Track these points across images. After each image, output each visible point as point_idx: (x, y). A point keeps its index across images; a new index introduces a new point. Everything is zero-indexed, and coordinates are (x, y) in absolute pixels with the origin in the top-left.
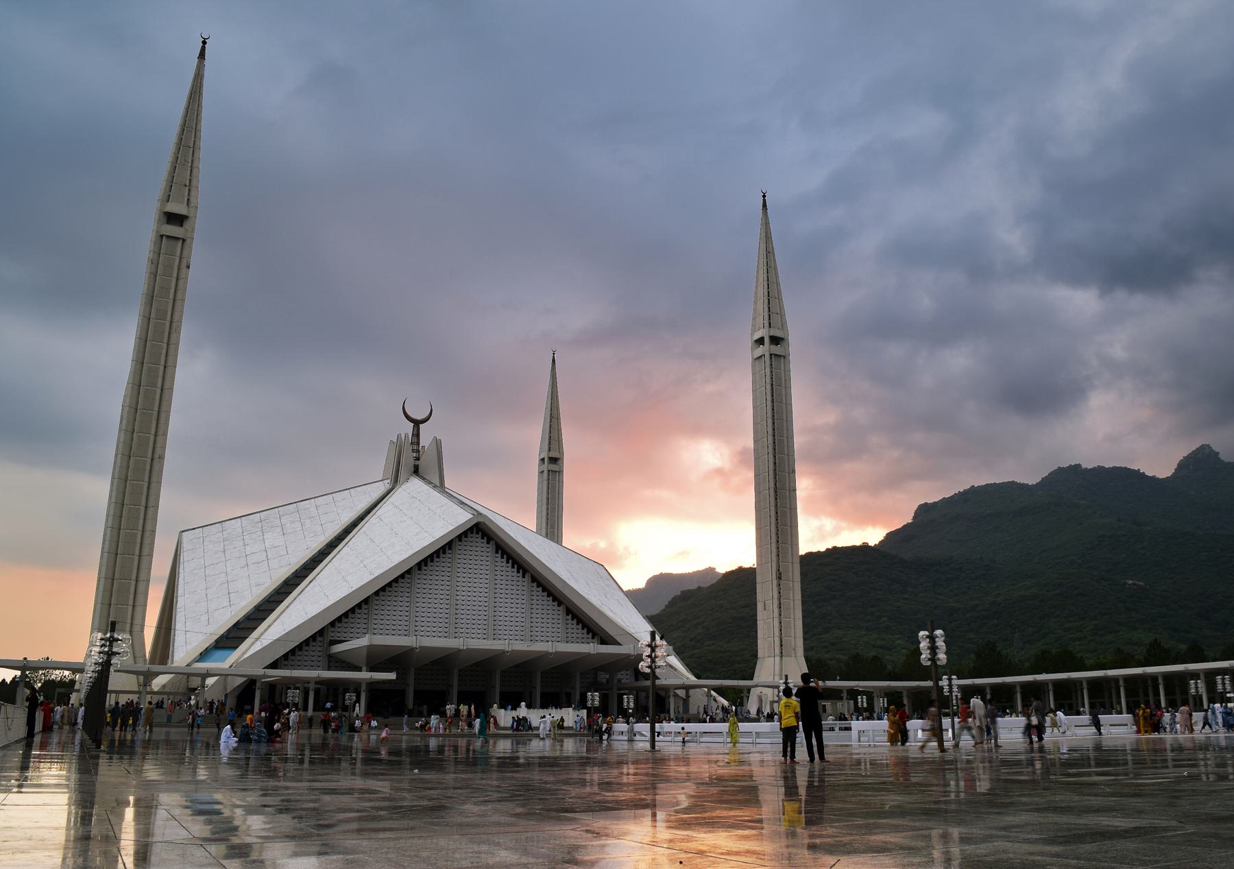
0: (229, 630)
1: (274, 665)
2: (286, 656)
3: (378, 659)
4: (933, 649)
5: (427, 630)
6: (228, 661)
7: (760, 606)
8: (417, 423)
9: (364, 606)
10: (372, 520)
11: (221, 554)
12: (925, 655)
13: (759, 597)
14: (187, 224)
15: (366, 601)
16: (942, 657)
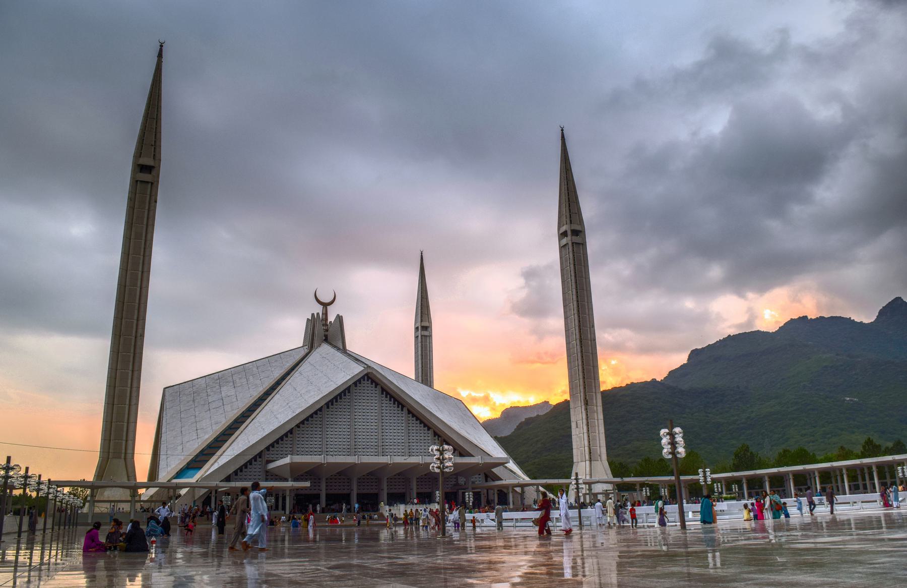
0: (197, 456)
1: (228, 479)
2: (236, 473)
3: (297, 472)
4: (673, 444)
5: (332, 452)
6: (195, 478)
7: (573, 425)
8: (325, 305)
9: (289, 435)
10: (295, 377)
11: (191, 403)
12: (666, 449)
13: (573, 419)
14: (154, 172)
15: (291, 431)
16: (681, 450)
